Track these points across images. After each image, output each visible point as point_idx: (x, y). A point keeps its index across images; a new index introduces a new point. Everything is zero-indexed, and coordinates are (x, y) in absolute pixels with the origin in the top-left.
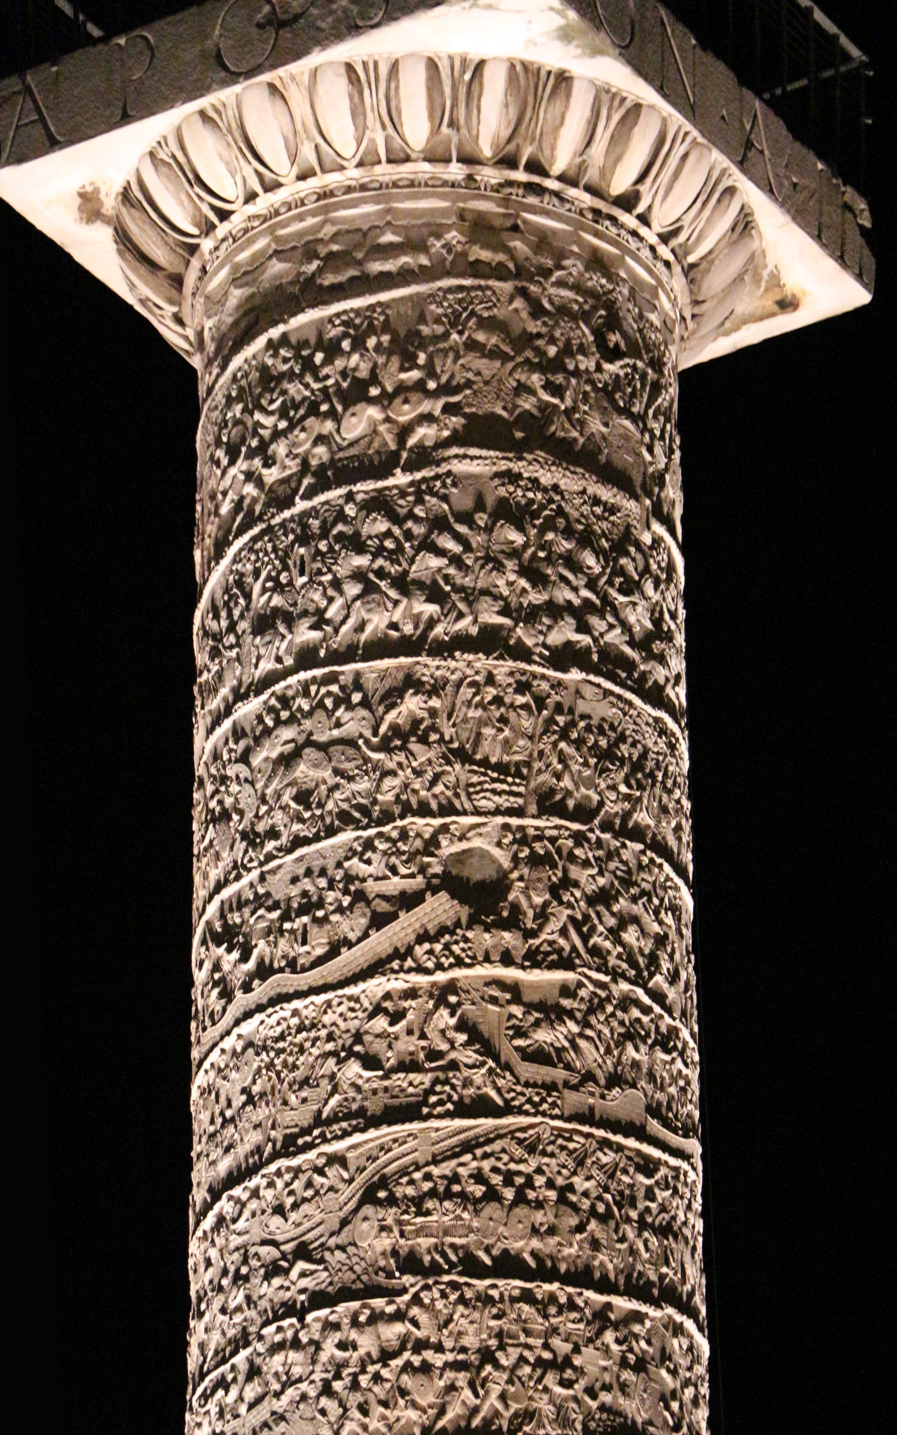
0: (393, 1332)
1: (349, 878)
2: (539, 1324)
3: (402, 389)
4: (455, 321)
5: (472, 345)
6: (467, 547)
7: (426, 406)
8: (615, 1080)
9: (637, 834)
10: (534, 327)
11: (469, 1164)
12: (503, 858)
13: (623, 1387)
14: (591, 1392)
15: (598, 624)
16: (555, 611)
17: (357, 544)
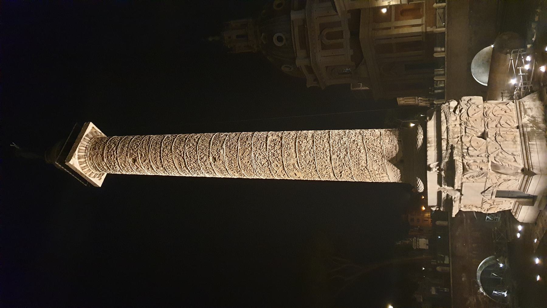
0: (168, 168)
1: (136, 169)
2: (164, 156)
3: (102, 165)
4: (96, 161)
5: (98, 160)
6: (111, 161)
7: (102, 163)
8: (146, 149)
9: (128, 146)
10: (95, 155)
11: (154, 162)
13: (168, 149)
14: (169, 152)
16: (114, 154)
17: (113, 168)
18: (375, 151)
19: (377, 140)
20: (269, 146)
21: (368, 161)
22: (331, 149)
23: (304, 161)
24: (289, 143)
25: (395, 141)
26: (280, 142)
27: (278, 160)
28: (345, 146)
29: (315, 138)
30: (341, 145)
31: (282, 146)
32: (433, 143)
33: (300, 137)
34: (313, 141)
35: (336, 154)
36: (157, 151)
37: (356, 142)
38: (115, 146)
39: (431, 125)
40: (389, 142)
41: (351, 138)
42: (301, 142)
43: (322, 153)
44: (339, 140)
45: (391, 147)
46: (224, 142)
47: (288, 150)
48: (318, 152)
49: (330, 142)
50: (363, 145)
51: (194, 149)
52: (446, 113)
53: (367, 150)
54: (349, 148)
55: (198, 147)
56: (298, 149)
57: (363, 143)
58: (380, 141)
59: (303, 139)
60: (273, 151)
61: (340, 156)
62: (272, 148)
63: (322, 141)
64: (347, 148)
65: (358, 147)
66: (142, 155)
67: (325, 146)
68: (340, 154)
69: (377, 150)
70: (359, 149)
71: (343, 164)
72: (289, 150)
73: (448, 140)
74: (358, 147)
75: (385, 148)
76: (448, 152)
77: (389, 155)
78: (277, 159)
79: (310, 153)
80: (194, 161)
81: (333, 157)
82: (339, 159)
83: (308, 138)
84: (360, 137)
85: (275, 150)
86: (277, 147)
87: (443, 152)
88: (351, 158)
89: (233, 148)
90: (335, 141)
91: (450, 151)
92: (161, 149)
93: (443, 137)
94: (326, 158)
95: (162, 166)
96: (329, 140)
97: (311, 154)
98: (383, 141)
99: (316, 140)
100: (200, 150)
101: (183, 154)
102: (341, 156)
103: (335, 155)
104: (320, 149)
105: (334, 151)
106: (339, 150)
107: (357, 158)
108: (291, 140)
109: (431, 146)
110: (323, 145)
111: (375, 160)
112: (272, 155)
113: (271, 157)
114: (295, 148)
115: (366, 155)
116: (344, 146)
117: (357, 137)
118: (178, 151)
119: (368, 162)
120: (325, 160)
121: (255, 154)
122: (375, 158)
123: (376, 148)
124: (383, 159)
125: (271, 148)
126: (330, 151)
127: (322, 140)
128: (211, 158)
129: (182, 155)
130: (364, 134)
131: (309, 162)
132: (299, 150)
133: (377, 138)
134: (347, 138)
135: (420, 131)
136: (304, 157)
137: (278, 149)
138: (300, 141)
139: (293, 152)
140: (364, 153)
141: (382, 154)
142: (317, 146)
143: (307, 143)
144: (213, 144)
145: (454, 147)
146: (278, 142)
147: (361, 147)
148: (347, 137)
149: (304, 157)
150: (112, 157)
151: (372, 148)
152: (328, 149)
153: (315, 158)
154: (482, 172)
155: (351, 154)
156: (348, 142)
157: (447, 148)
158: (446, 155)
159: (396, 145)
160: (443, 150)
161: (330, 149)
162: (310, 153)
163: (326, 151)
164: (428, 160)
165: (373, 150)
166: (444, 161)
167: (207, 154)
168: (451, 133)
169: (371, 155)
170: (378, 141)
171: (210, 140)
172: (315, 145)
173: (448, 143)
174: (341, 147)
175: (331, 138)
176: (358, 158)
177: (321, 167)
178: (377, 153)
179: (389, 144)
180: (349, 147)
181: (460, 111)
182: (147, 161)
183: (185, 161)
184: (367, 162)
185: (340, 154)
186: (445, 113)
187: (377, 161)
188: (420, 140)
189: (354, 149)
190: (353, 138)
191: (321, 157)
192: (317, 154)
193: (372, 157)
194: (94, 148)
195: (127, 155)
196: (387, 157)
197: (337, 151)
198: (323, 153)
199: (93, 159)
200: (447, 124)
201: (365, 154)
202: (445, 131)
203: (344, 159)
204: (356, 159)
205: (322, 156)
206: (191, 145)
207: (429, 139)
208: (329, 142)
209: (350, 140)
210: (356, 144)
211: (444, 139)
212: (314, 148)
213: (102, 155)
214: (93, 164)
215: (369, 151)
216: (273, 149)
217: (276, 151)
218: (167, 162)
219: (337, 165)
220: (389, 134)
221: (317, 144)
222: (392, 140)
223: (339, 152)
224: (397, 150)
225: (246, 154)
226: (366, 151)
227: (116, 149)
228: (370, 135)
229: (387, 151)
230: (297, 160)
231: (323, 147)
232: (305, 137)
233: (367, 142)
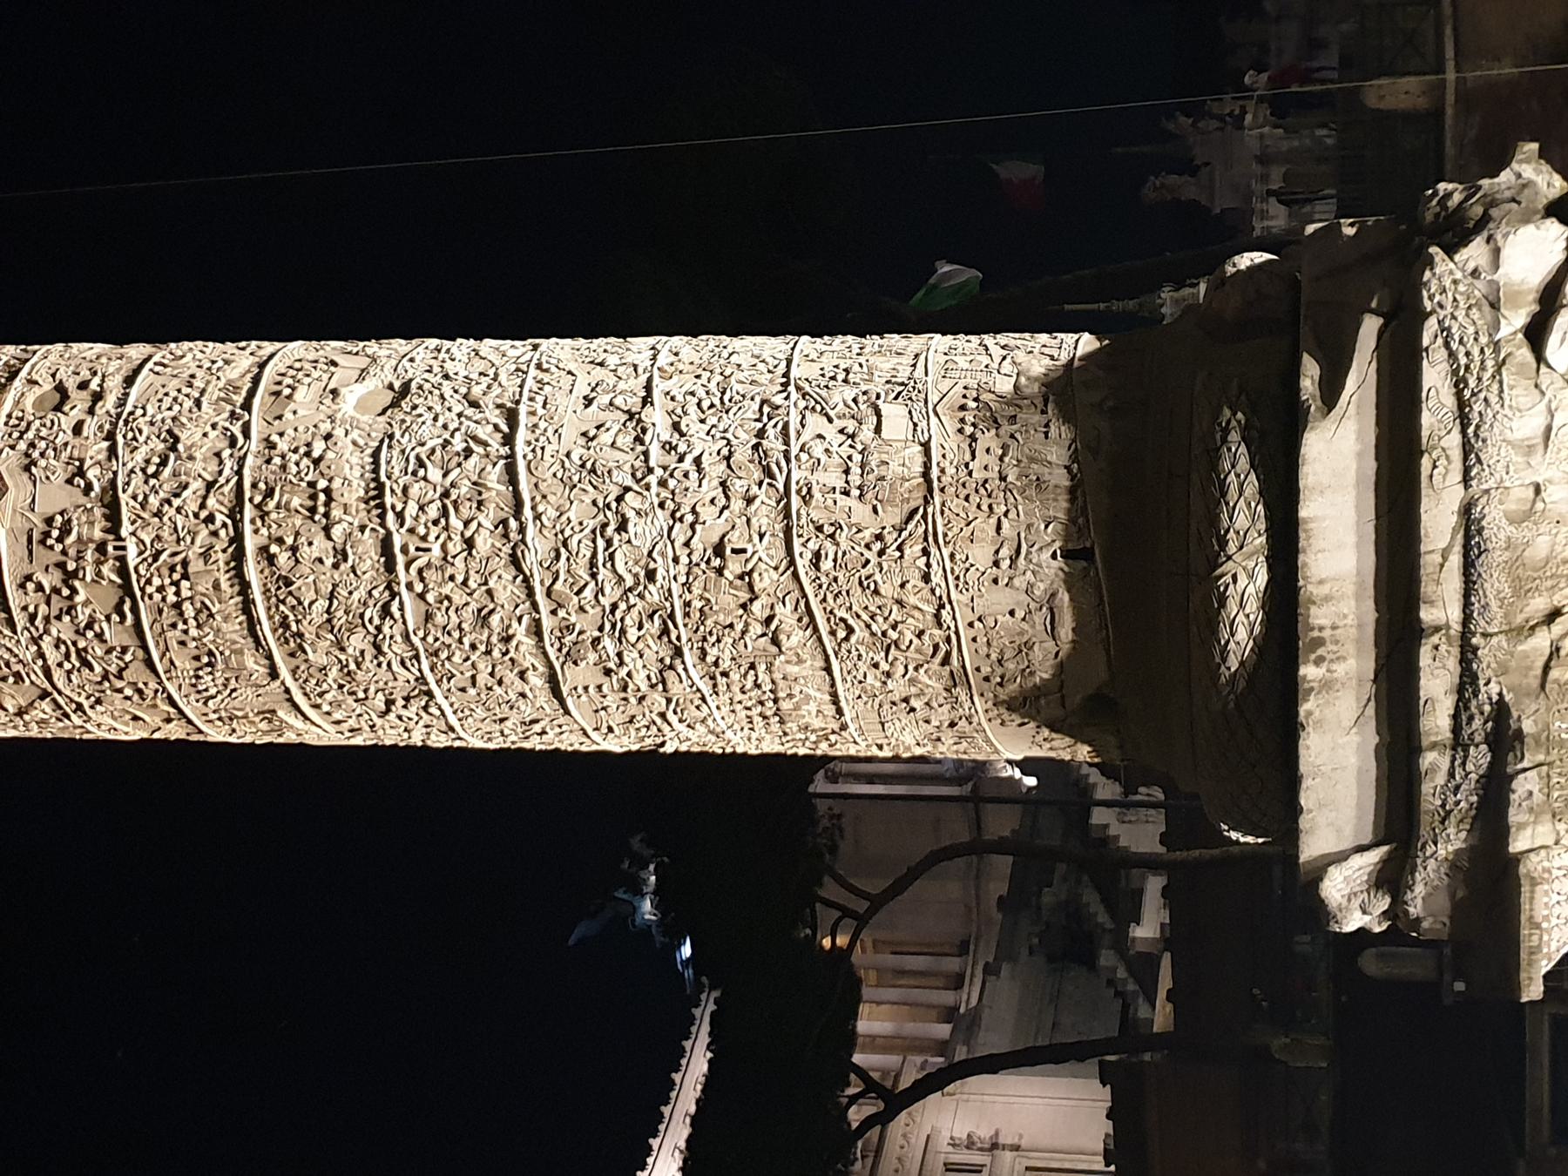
18: (896, 643)
19: (900, 548)
20: (22, 586)
21: (843, 704)
22: (547, 623)
23: (350, 700)
24: (185, 563)
25: (1046, 555)
28: (654, 594)
29: (400, 516)
30: (618, 593)
31: (126, 588)
32: (1350, 648)
33: (271, 504)
34: (386, 546)
35: (592, 657)
37: (734, 567)
40: (996, 564)
41: (689, 518)
42: (283, 559)
43: (473, 647)
44: (601, 543)
45: (1012, 613)
47: (192, 623)
48: (447, 640)
49: (530, 561)
50: (797, 594)
52: (1463, 360)
53: (833, 633)
54: (687, 615)
56: (270, 618)
57: (796, 575)
58: (926, 552)
59: (298, 521)
61: (623, 672)
62: (48, 603)
64: (672, 616)
67: (489, 592)
68: (619, 655)
69: (909, 636)
70: (769, 620)
71: (663, 715)
72: (199, 626)
73: (1467, 653)
74: (756, 607)
75: (971, 617)
76: (1470, 767)
77: (999, 671)
79: (377, 647)
81: (571, 677)
82: (625, 689)
83: (336, 513)
84: (765, 513)
85: (82, 619)
86: (92, 598)
87: (1428, 759)
88: (715, 686)
90: (565, 544)
91: (1480, 757)
93: (1427, 615)
94: (518, 681)
96: (514, 536)
97: (390, 655)
98: (952, 556)
99: (411, 531)
102: (629, 675)
103: (583, 664)
104: (455, 619)
105: (568, 639)
106: (608, 626)
107: (758, 686)
108: (194, 534)
109: (1327, 685)
110: (472, 584)
111: (897, 699)
112: (67, 656)
113: (69, 672)
114: (247, 606)
115: (828, 669)
116: (641, 596)
117: (737, 505)
119: (846, 710)
120: (513, 696)
122: (898, 687)
123: (896, 615)
125: (43, 609)
126: (537, 630)
127: (457, 538)
130: (795, 476)
131: (389, 703)
132: (285, 624)
133: (897, 521)
134: (662, 518)
135: (1241, 521)
136: (334, 673)
137: (108, 618)
138: (274, 549)
139: (235, 637)
140: (813, 657)
141: (946, 661)
142: (430, 597)
143: (336, 566)
145: (1519, 735)
146: (90, 555)
147: (779, 609)
148: (662, 505)
149: (334, 673)
151: (865, 617)
152: (520, 619)
153: (427, 684)
155: (710, 659)
156: (676, 560)
157: (1456, 730)
158: (1451, 799)
159: (1053, 595)
160: (1425, 743)
161: (537, 623)
162: (377, 647)
163: (507, 639)
164: (1304, 821)
165: (873, 634)
166: (1430, 850)
168: (1494, 584)
169: (862, 667)
170: (907, 551)
172: (410, 586)
173: (1467, 681)
174: (623, 606)
175: (527, 513)
176: (767, 687)
178: (911, 654)
179: (995, 581)
180: (687, 604)
184: (840, 712)
185: (619, 655)
186: (1452, 355)
187: (914, 703)
188: (1242, 606)
189: (731, 626)
190: (708, 513)
191: (473, 677)
192: (436, 654)
193: (870, 679)
196: (987, 679)
197: (596, 641)
198: (483, 648)
200: (1466, 480)
201: (820, 663)
202: (1445, 555)
203: (660, 687)
204: (755, 693)
205: (484, 667)
207: (1313, 610)
208: (515, 561)
209: (687, 544)
210: (739, 582)
211: (1437, 629)
212: (401, 609)
215: (847, 639)
216: (67, 619)
217: (90, 634)
220: (994, 484)
221: (422, 579)
222: (1018, 552)
223: (608, 644)
224: (1066, 632)
226: (820, 639)
228: (846, 493)
229: (989, 644)
230: (287, 691)
231: (474, 606)
232: (314, 497)
233: (827, 565)
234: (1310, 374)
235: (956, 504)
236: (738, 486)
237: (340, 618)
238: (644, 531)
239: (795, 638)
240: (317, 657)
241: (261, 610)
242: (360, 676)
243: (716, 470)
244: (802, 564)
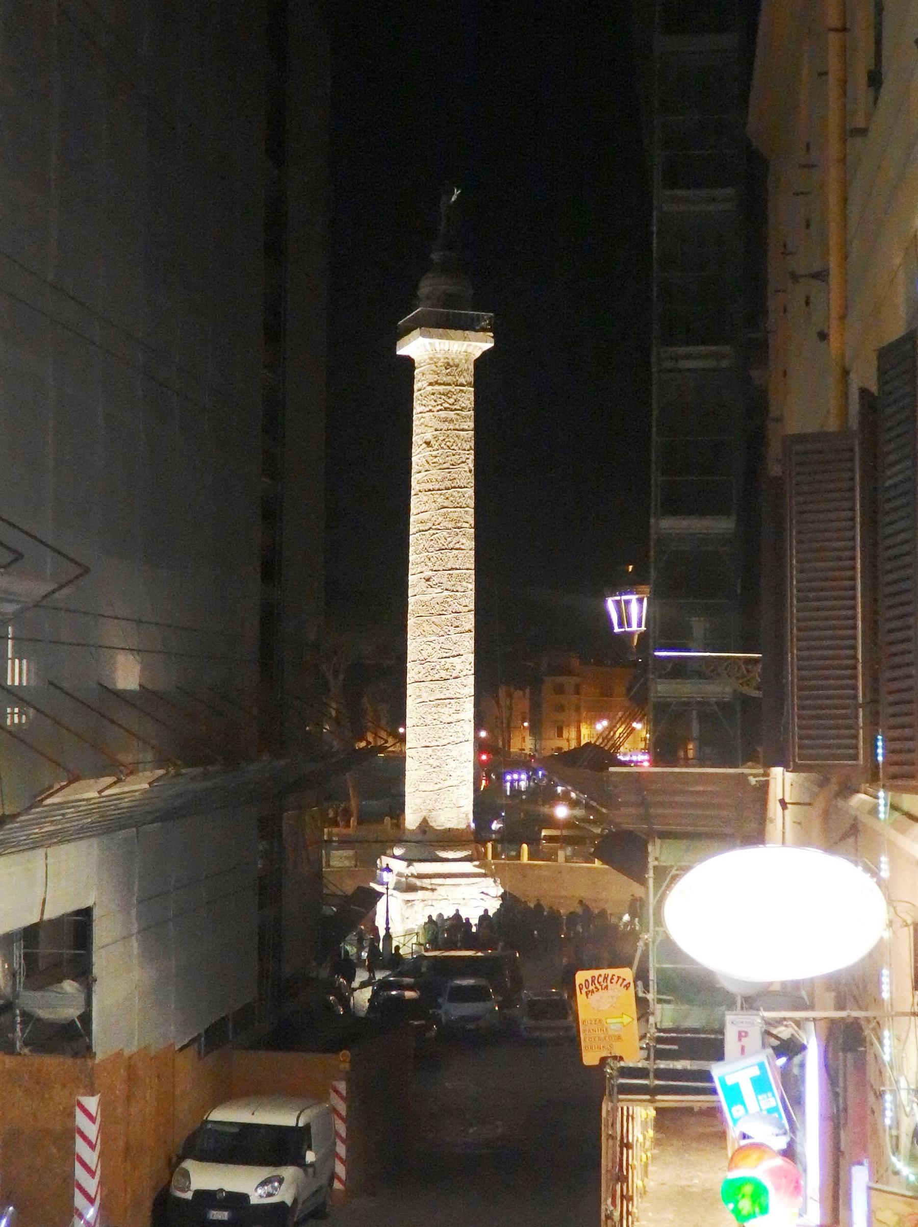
8: (444, 463)
9: (450, 429)
11: (425, 478)
12: (431, 438)
15: (444, 404)
26: (451, 676)
27: (426, 675)
28: (444, 765)
36: (440, 483)
37: (448, 778)
38: (450, 404)
39: (468, 867)
42: (450, 706)
46: (453, 591)
51: (443, 545)
55: (446, 551)
60: (438, 667)
63: (450, 734)
65: (442, 782)
66: (436, 457)
78: (428, 674)
80: (426, 546)
86: (443, 674)
87: (428, 880)
89: (443, 608)
91: (430, 887)
92: (443, 490)
95: (420, 491)
100: (441, 555)
101: (436, 529)
118: (441, 519)
121: (434, 642)
122: (428, 802)
124: (427, 811)
128: (431, 573)
129: (434, 527)
144: (450, 574)
146: (450, 674)
150: (433, 403)
154: (405, 918)
167: (435, 568)
171: (457, 569)
177: (418, 733)
181: (482, 899)
182: (427, 467)
183: (426, 531)
194: (448, 364)
195: (436, 430)
199: (430, 364)
204: (426, 779)
206: (449, 539)
208: (449, 743)
213: (437, 383)
214: (424, 362)
218: (425, 500)
219: (420, 754)
223: (435, 757)
225: (434, 627)
227: (446, 409)
234: (477, 863)
235: (456, 812)
236: (459, 778)
237: (440, 714)
238: (453, 764)
239: (437, 787)
240: (433, 709)
241: (441, 701)
242: (429, 715)
243: (461, 775)
244: (449, 788)
